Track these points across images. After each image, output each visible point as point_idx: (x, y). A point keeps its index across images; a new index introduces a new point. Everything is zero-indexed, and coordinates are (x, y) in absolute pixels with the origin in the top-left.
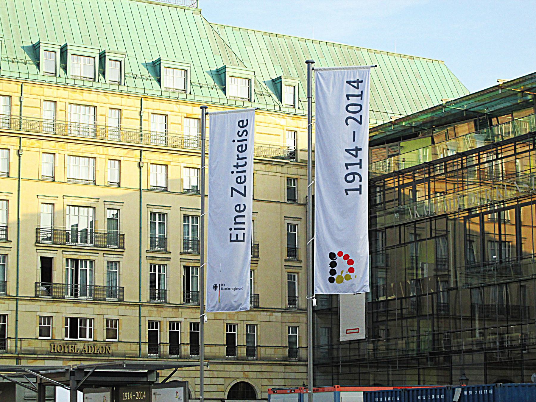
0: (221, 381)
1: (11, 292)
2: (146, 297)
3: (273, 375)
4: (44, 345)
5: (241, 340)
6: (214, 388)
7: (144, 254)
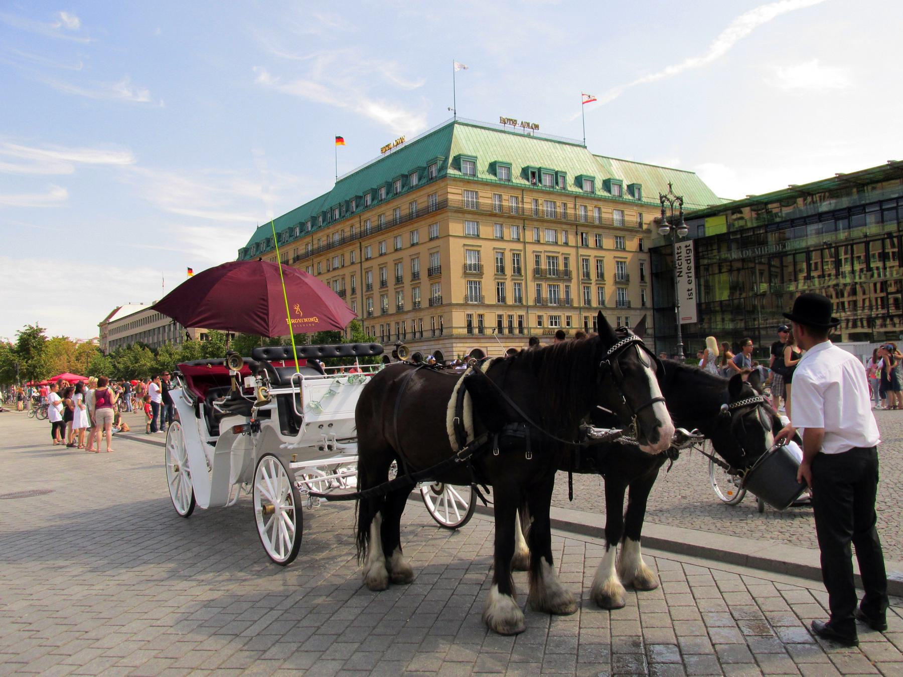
1: (524, 303)
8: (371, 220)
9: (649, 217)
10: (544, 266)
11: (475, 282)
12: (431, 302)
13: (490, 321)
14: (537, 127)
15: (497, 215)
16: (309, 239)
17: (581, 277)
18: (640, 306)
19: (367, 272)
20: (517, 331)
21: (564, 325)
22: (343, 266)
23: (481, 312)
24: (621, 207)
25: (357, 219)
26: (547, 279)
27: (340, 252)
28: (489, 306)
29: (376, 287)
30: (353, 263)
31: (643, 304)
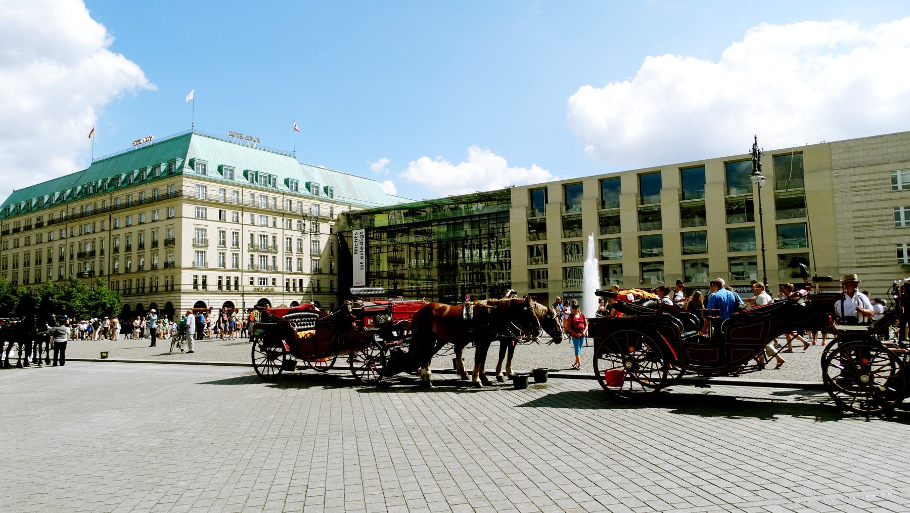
1: (240, 268)
4: (251, 289)
8: (121, 197)
9: (339, 210)
10: (257, 241)
11: (202, 252)
12: (167, 265)
13: (212, 282)
14: (258, 140)
15: (222, 206)
16: (63, 207)
17: (285, 250)
18: (328, 271)
19: (115, 239)
20: (233, 288)
21: (270, 284)
22: (94, 232)
25: (109, 196)
26: (258, 251)
27: (91, 220)
29: (122, 249)
30: (103, 230)
31: (331, 270)
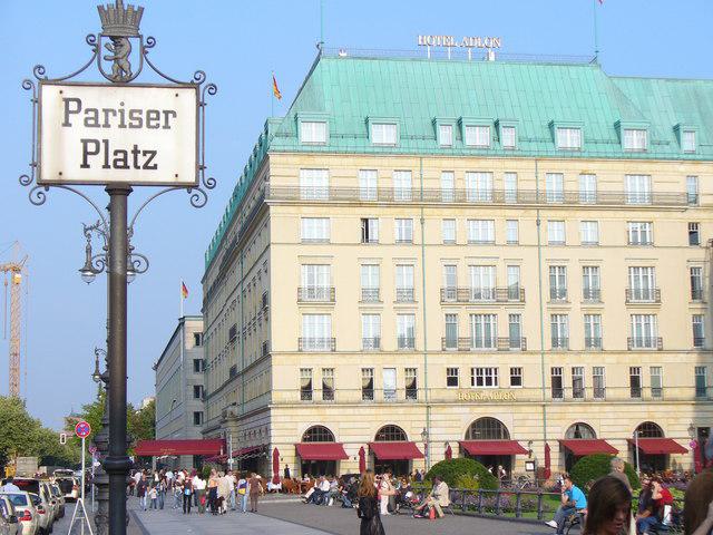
0: (625, 422)
1: (419, 345)
2: (548, 345)
3: (680, 415)
5: (645, 381)
6: (620, 429)
7: (545, 306)
23: (329, 361)
24: (645, 167)
28: (344, 354)
